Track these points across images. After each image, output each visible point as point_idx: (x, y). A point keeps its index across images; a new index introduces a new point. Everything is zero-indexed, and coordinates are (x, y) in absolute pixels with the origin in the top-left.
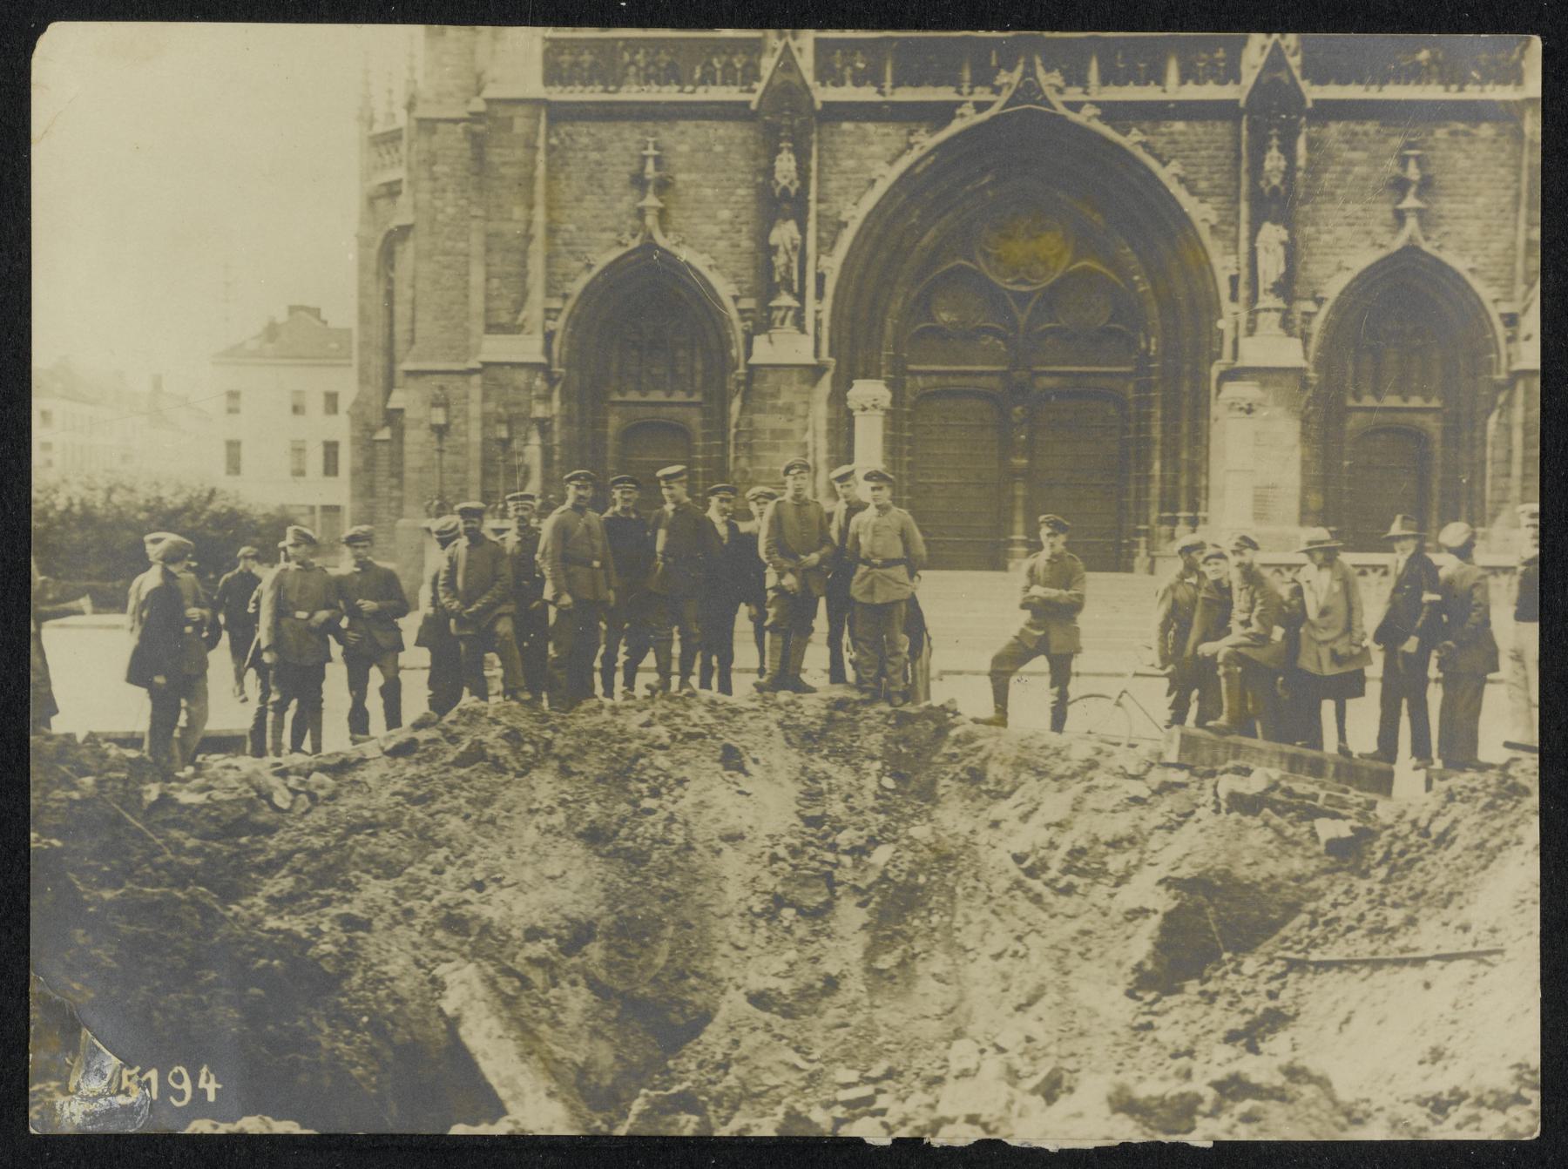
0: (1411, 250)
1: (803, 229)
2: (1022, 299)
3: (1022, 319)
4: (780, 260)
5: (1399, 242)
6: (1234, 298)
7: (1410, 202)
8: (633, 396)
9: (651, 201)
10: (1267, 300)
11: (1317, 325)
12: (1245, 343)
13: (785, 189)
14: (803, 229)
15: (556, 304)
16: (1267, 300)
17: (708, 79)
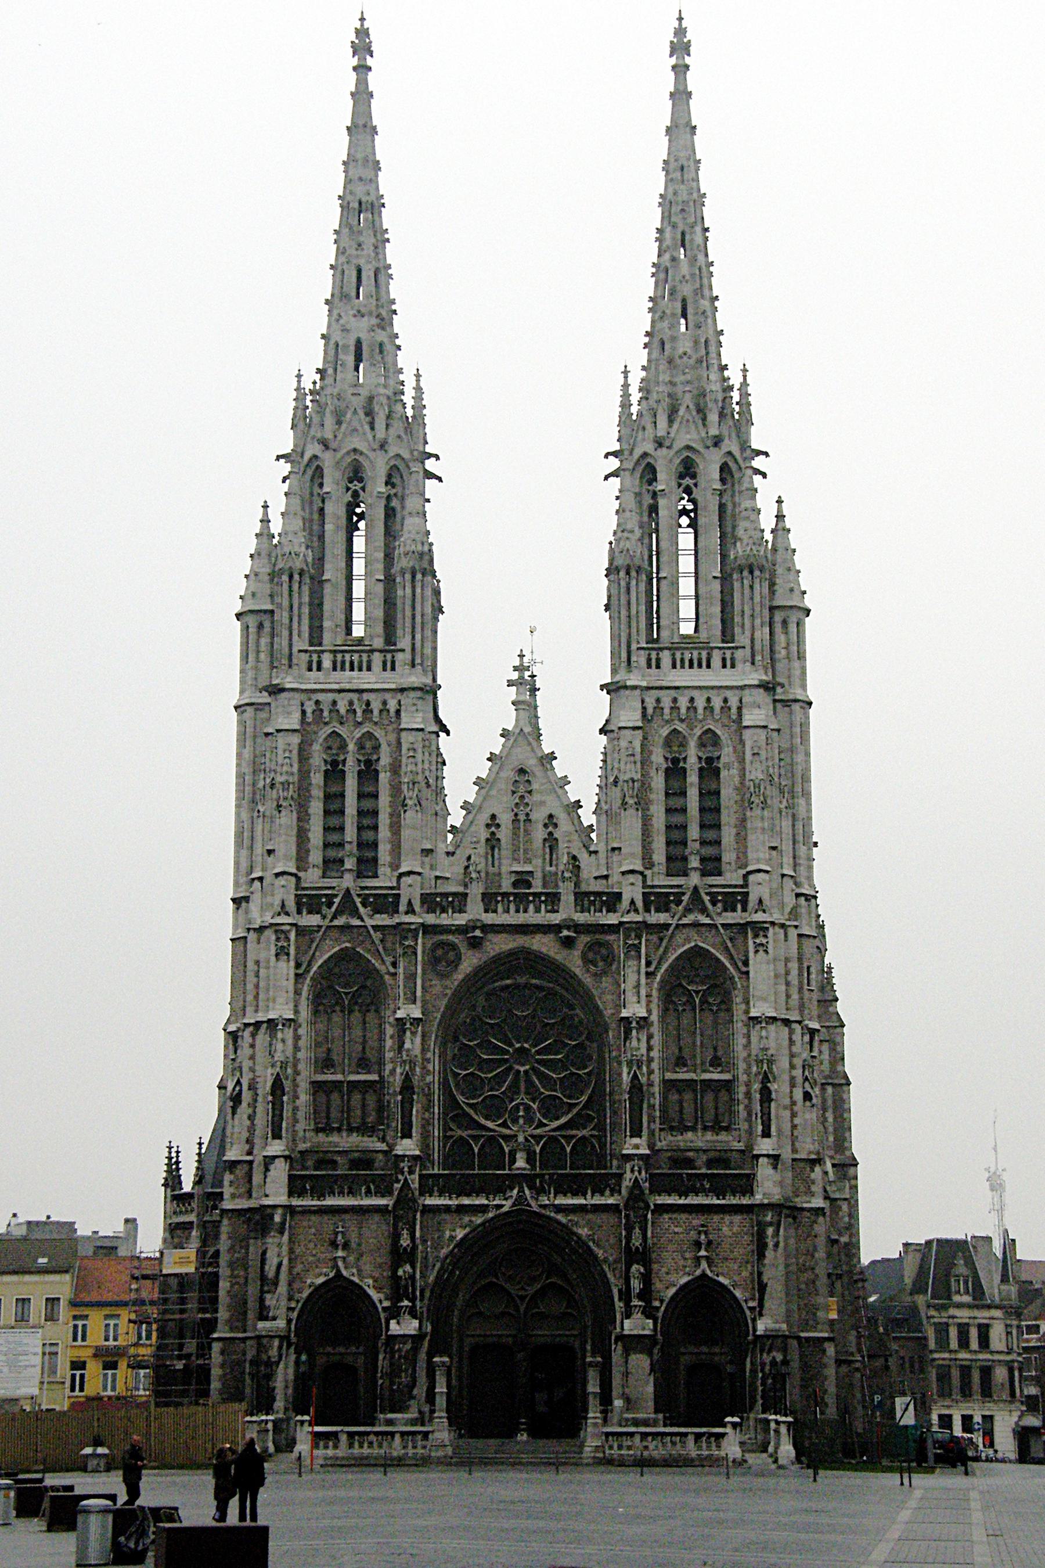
0: (704, 1275)
1: (413, 1267)
2: (522, 1298)
3: (522, 1309)
4: (403, 1283)
5: (698, 1272)
6: (620, 1299)
7: (703, 1253)
8: (329, 1349)
9: (340, 1253)
10: (635, 1302)
11: (660, 1314)
12: (627, 1322)
13: (405, 1249)
14: (413, 1267)
15: (293, 1305)
16: (635, 1302)
17: (368, 1192)
